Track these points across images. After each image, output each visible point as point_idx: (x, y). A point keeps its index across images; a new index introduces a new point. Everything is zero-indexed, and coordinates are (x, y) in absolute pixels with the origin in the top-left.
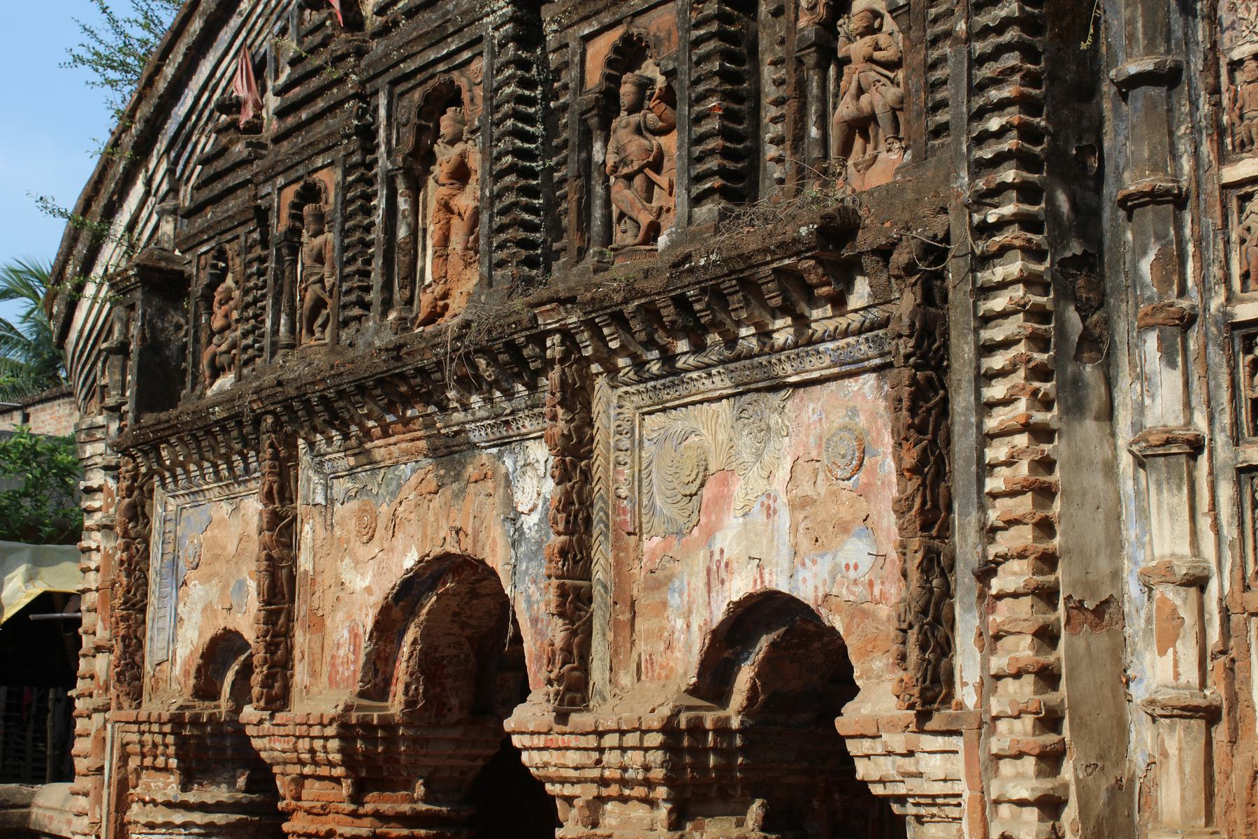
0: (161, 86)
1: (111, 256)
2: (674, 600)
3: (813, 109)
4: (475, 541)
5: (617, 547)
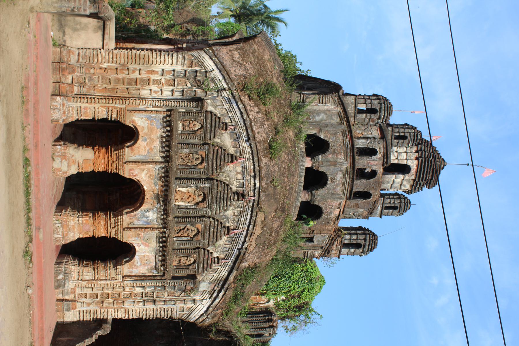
0: (239, 103)
2: (136, 239)
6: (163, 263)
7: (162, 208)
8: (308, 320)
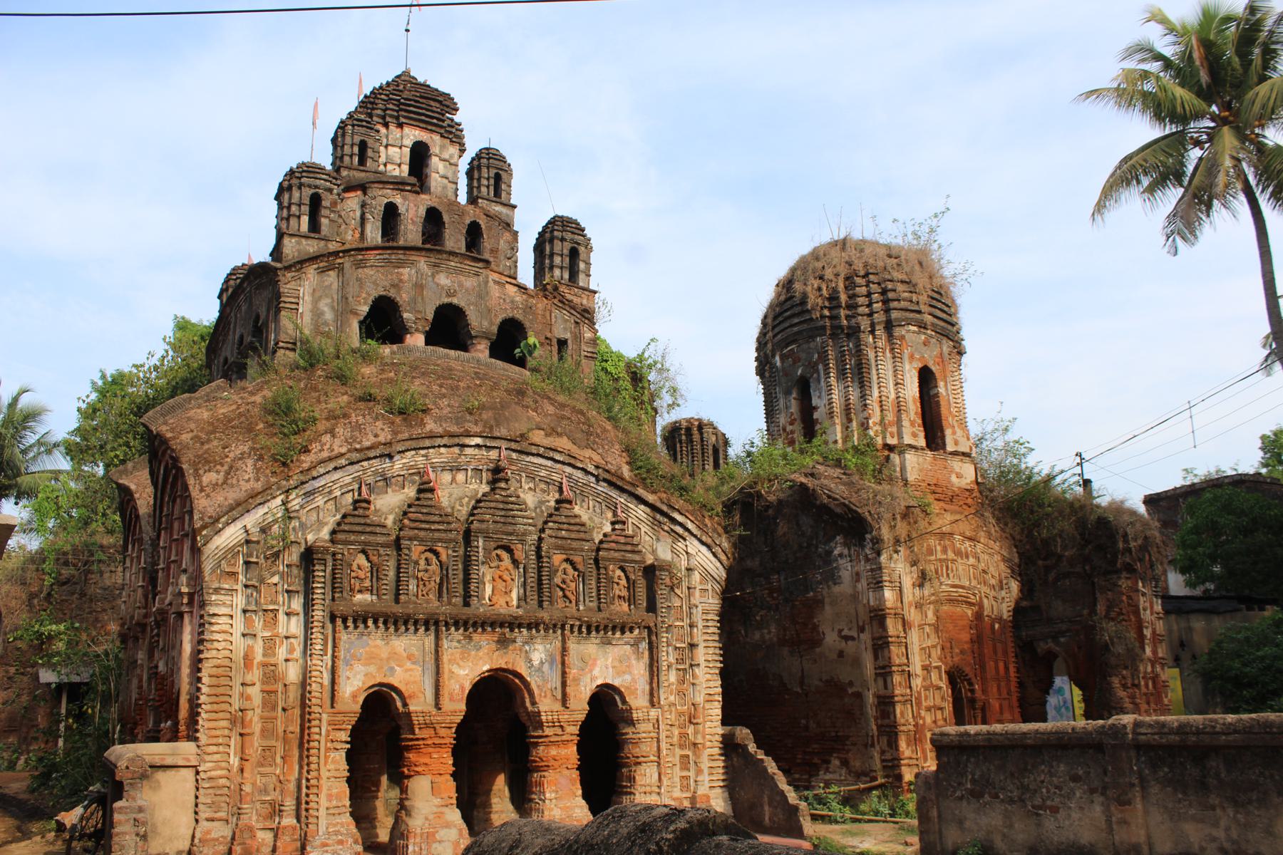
0: (315, 474)
6: (626, 629)
7: (524, 631)
8: (659, 366)
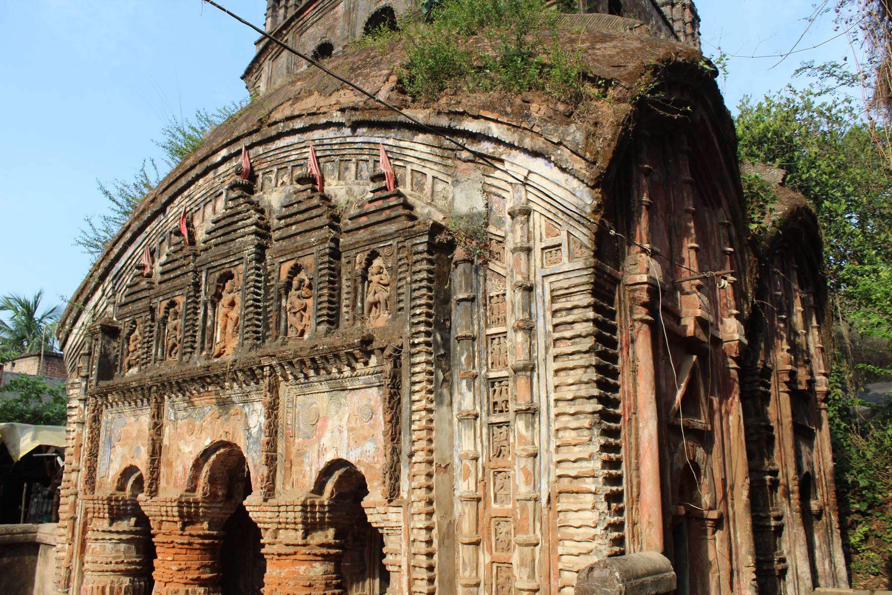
0: (112, 256)
1: (85, 318)
2: (306, 460)
3: (359, 297)
4: (233, 436)
5: (286, 441)
